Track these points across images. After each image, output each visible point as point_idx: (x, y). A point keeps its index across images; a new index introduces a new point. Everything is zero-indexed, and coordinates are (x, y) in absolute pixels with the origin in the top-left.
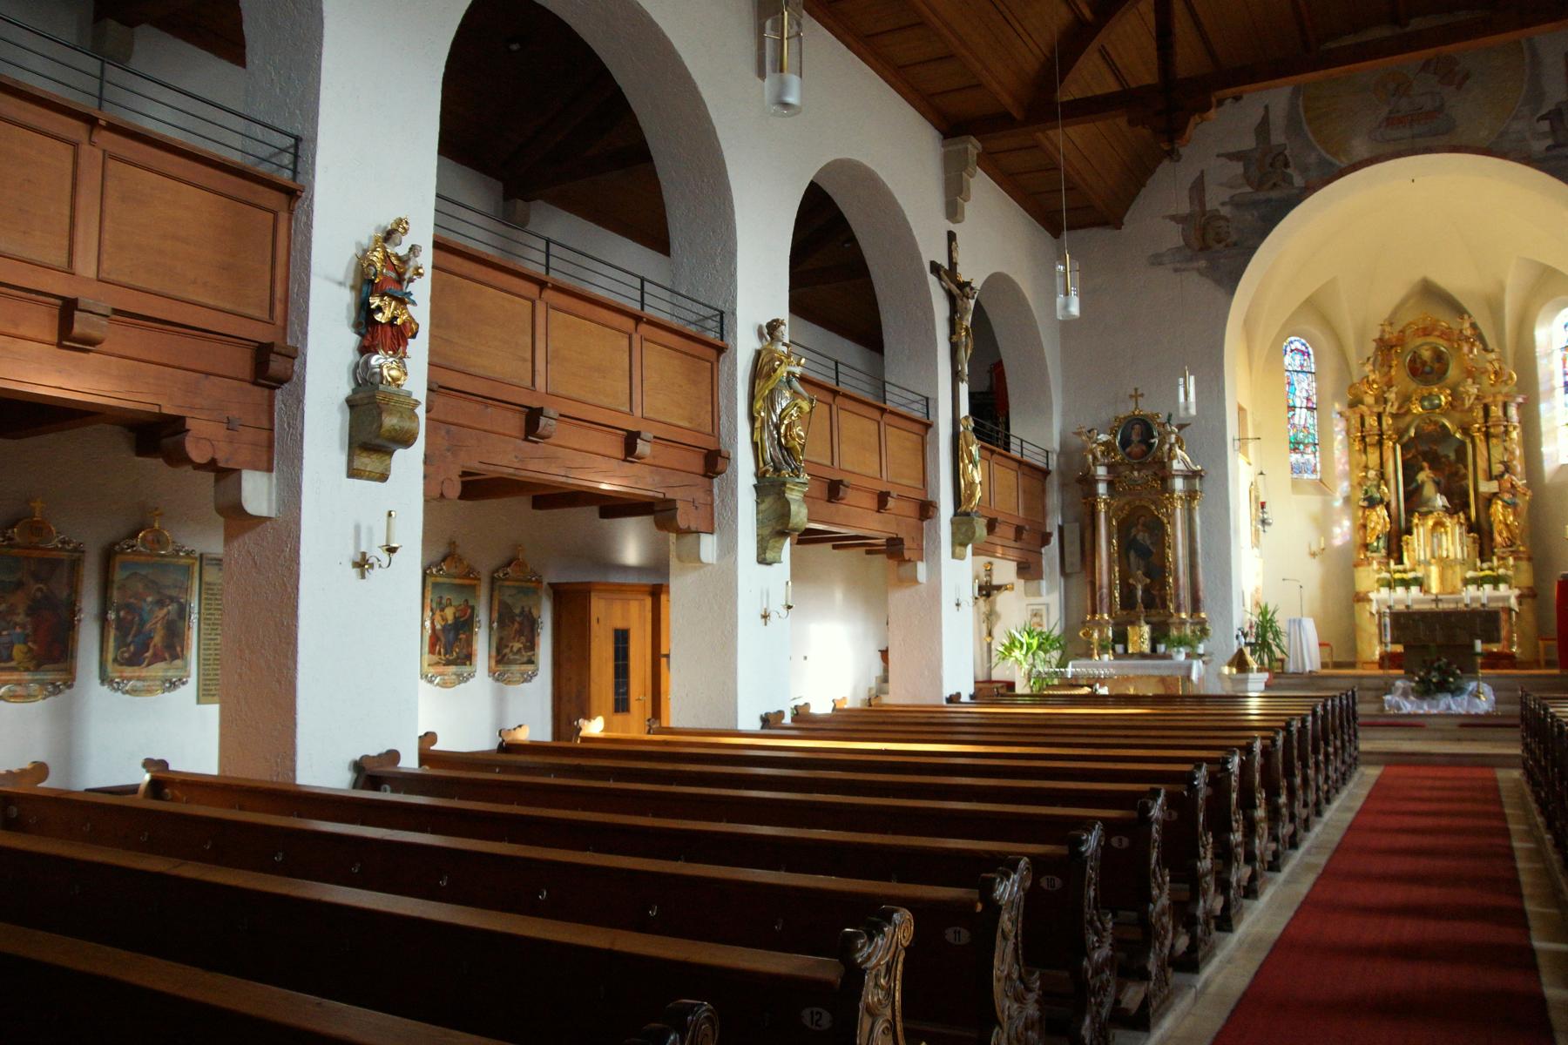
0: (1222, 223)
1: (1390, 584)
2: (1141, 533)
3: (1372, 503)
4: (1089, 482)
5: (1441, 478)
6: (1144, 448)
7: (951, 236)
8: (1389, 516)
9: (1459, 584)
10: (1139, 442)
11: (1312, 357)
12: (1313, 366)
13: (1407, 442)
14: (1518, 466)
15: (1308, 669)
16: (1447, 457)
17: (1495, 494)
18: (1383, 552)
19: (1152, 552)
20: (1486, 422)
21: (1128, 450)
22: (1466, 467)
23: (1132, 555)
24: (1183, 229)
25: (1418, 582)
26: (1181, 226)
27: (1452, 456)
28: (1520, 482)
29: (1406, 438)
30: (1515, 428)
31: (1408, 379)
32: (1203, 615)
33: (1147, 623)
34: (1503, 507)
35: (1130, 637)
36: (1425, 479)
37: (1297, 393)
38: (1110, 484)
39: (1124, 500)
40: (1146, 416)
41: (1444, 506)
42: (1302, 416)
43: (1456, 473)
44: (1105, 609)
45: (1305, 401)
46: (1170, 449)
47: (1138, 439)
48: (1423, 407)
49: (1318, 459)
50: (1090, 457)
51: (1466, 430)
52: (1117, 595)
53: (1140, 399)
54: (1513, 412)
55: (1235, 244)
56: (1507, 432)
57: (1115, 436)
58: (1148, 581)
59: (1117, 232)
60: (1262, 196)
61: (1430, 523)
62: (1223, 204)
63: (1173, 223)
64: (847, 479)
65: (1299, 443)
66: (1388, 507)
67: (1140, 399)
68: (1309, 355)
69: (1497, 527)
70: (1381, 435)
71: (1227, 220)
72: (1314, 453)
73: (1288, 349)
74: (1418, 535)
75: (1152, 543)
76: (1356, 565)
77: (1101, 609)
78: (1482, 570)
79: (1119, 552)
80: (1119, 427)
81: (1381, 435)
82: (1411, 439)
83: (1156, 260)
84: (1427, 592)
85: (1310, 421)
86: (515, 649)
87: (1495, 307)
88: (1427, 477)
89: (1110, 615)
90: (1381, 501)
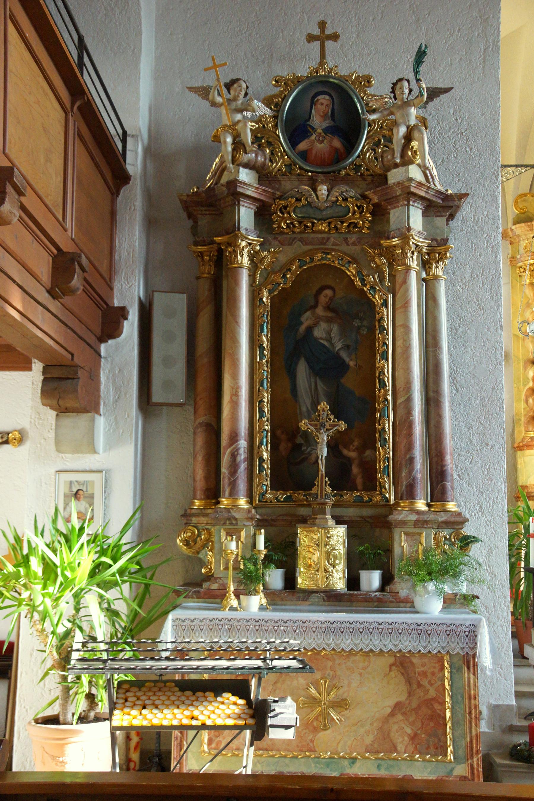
2: (323, 325)
6: (337, 143)
10: (327, 131)
21: (303, 146)
32: (451, 506)
33: (339, 521)
35: (302, 551)
40: (344, 79)
44: (242, 485)
46: (408, 138)
47: (325, 124)
50: (229, 140)
52: (265, 455)
53: (329, 44)
58: (343, 426)
67: (329, 44)
75: (347, 347)
77: (233, 485)
79: (272, 363)
89: (250, 501)
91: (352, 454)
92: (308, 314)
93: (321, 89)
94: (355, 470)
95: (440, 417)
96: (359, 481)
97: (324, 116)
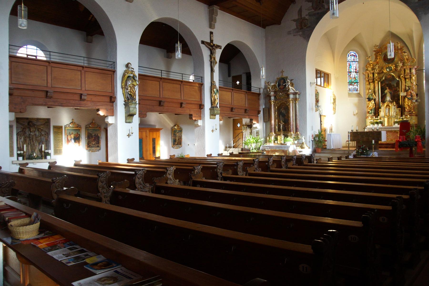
0: (306, 21)
1: (373, 123)
2: (283, 110)
3: (369, 99)
4: (270, 97)
5: (392, 92)
7: (211, 33)
8: (375, 103)
9: (393, 123)
11: (357, 57)
12: (358, 59)
13: (383, 81)
14: (415, 88)
15: (332, 148)
16: (394, 85)
17: (406, 96)
18: (373, 114)
19: (285, 115)
20: (404, 74)
21: (280, 87)
22: (399, 88)
23: (281, 116)
24: (296, 24)
25: (381, 123)
26: (295, 23)
27: (395, 85)
28: (414, 93)
29: (382, 80)
30: (414, 76)
31: (383, 62)
32: (298, 133)
33: (283, 135)
34: (408, 100)
36: (387, 92)
37: (352, 68)
38: (275, 97)
39: (279, 101)
41: (389, 100)
42: (353, 75)
43: (396, 90)
45: (355, 70)
48: (387, 70)
49: (358, 87)
50: (268, 90)
51: (399, 77)
52: (277, 127)
54: (413, 71)
55: (309, 27)
56: (411, 77)
57: (277, 84)
59: (279, 26)
60: (317, 12)
61: (385, 105)
62: (306, 15)
63: (294, 22)
64: (163, 100)
65: (352, 83)
66: (375, 100)
68: (356, 56)
69: (406, 106)
70: (374, 79)
71: (307, 19)
72: (357, 85)
73: (350, 55)
74: (382, 109)
75: (286, 113)
76: (366, 118)
78: (400, 119)
80: (277, 81)
81: (374, 79)
82: (383, 80)
83: (289, 33)
84: (384, 125)
85: (356, 76)
86: (93, 144)
87: (411, 38)
88: (388, 91)
90: (373, 99)
91: (287, 127)
92: (281, 109)
93: (281, 80)
94: (287, 129)
95: (297, 121)
96: (287, 130)
97: (282, 83)
